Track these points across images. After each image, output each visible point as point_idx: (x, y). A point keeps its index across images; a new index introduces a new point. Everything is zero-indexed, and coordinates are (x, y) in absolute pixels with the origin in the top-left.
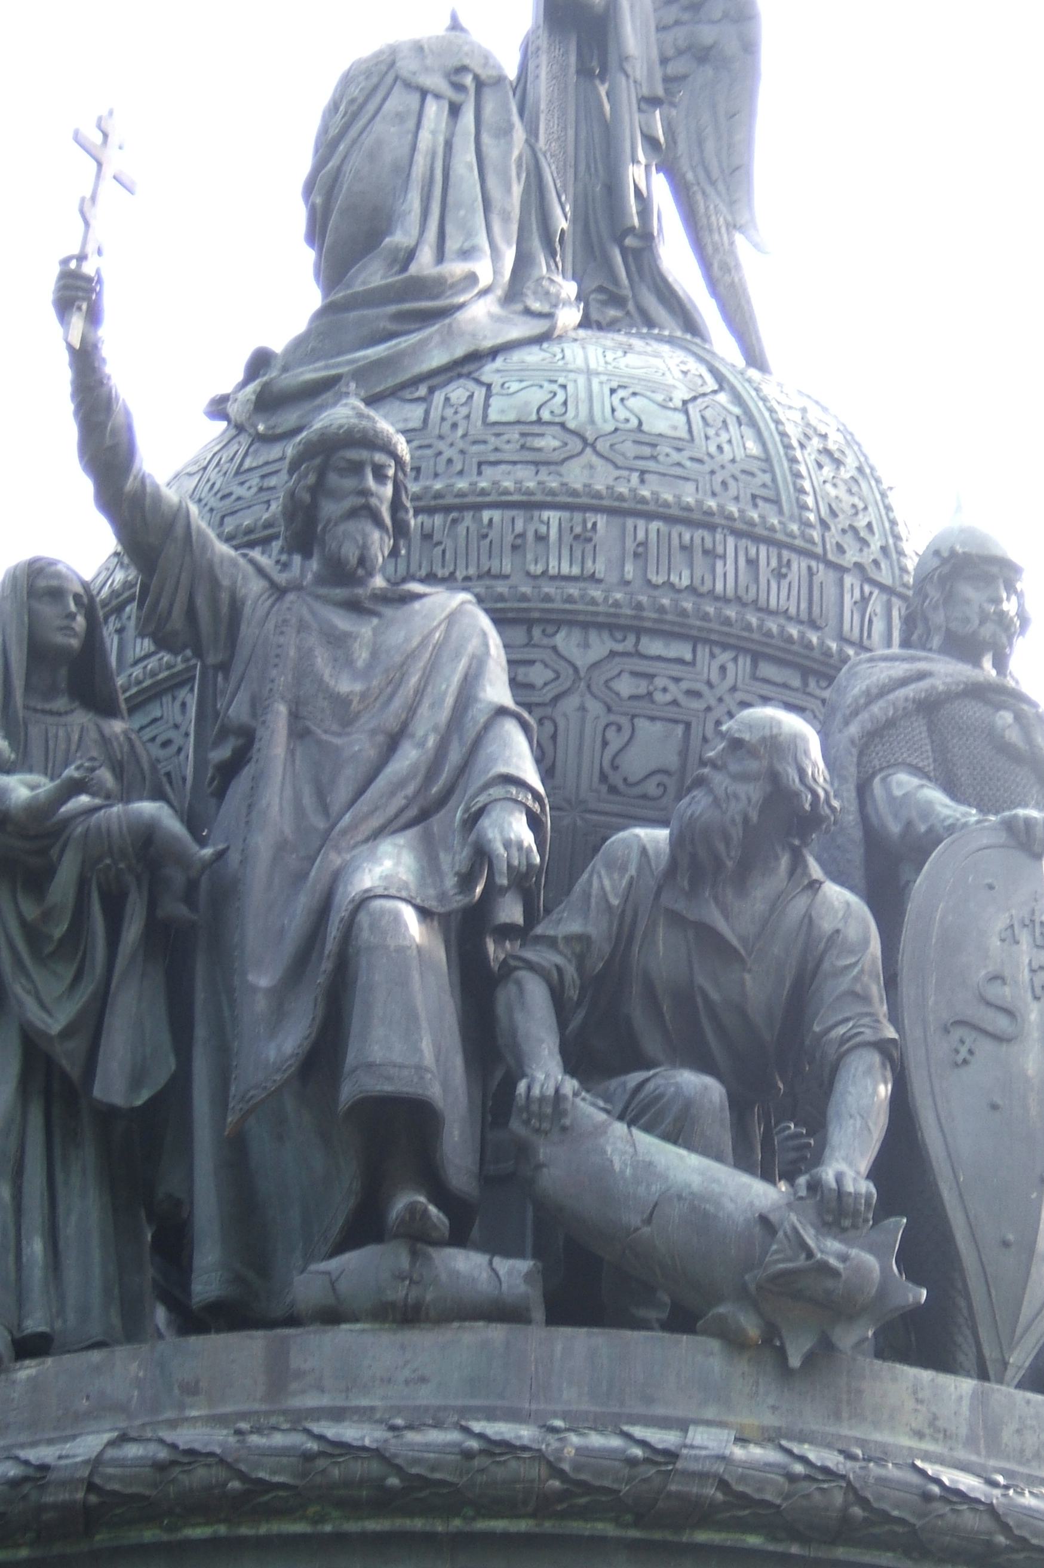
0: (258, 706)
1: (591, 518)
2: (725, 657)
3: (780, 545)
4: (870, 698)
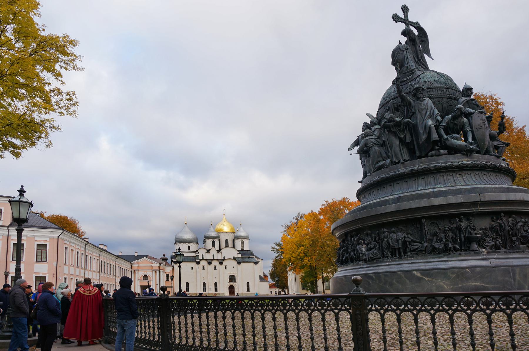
0: (415, 110)
1: (433, 89)
2: (445, 99)
3: (448, 89)
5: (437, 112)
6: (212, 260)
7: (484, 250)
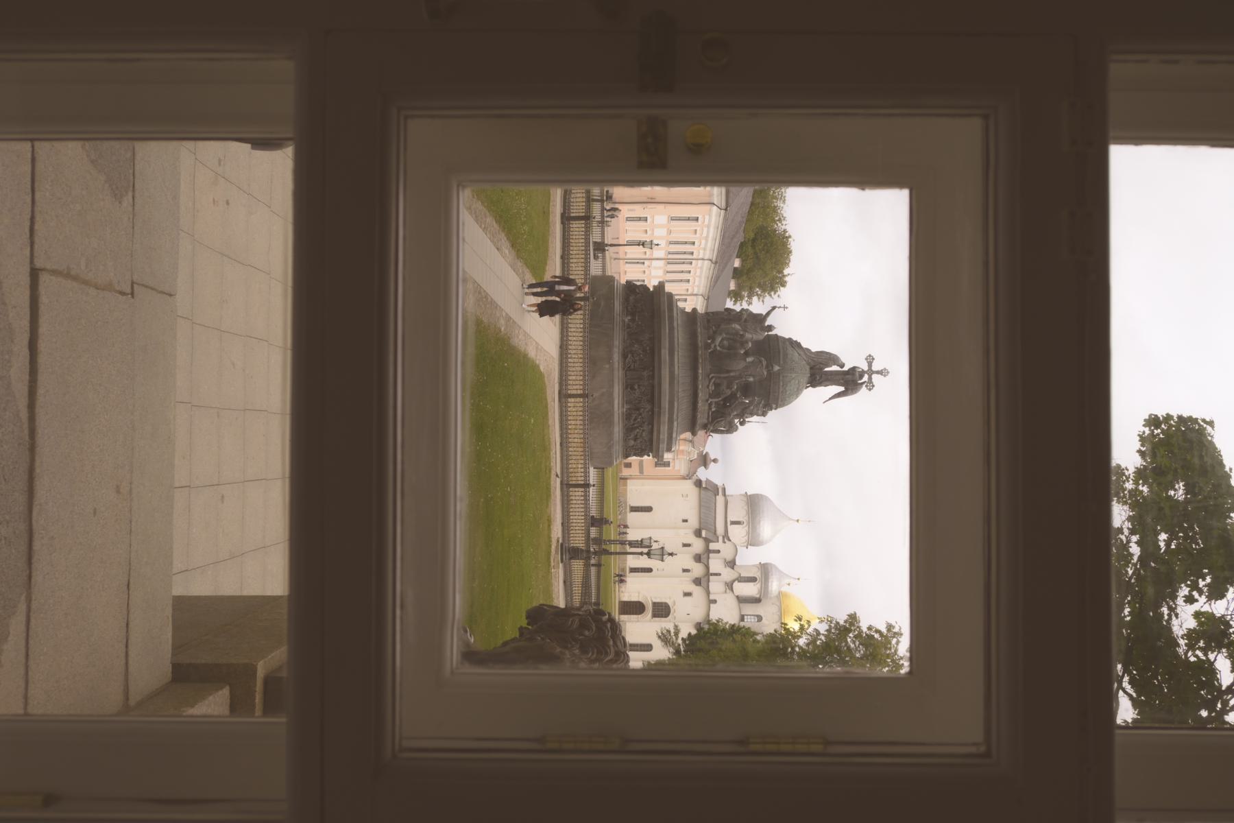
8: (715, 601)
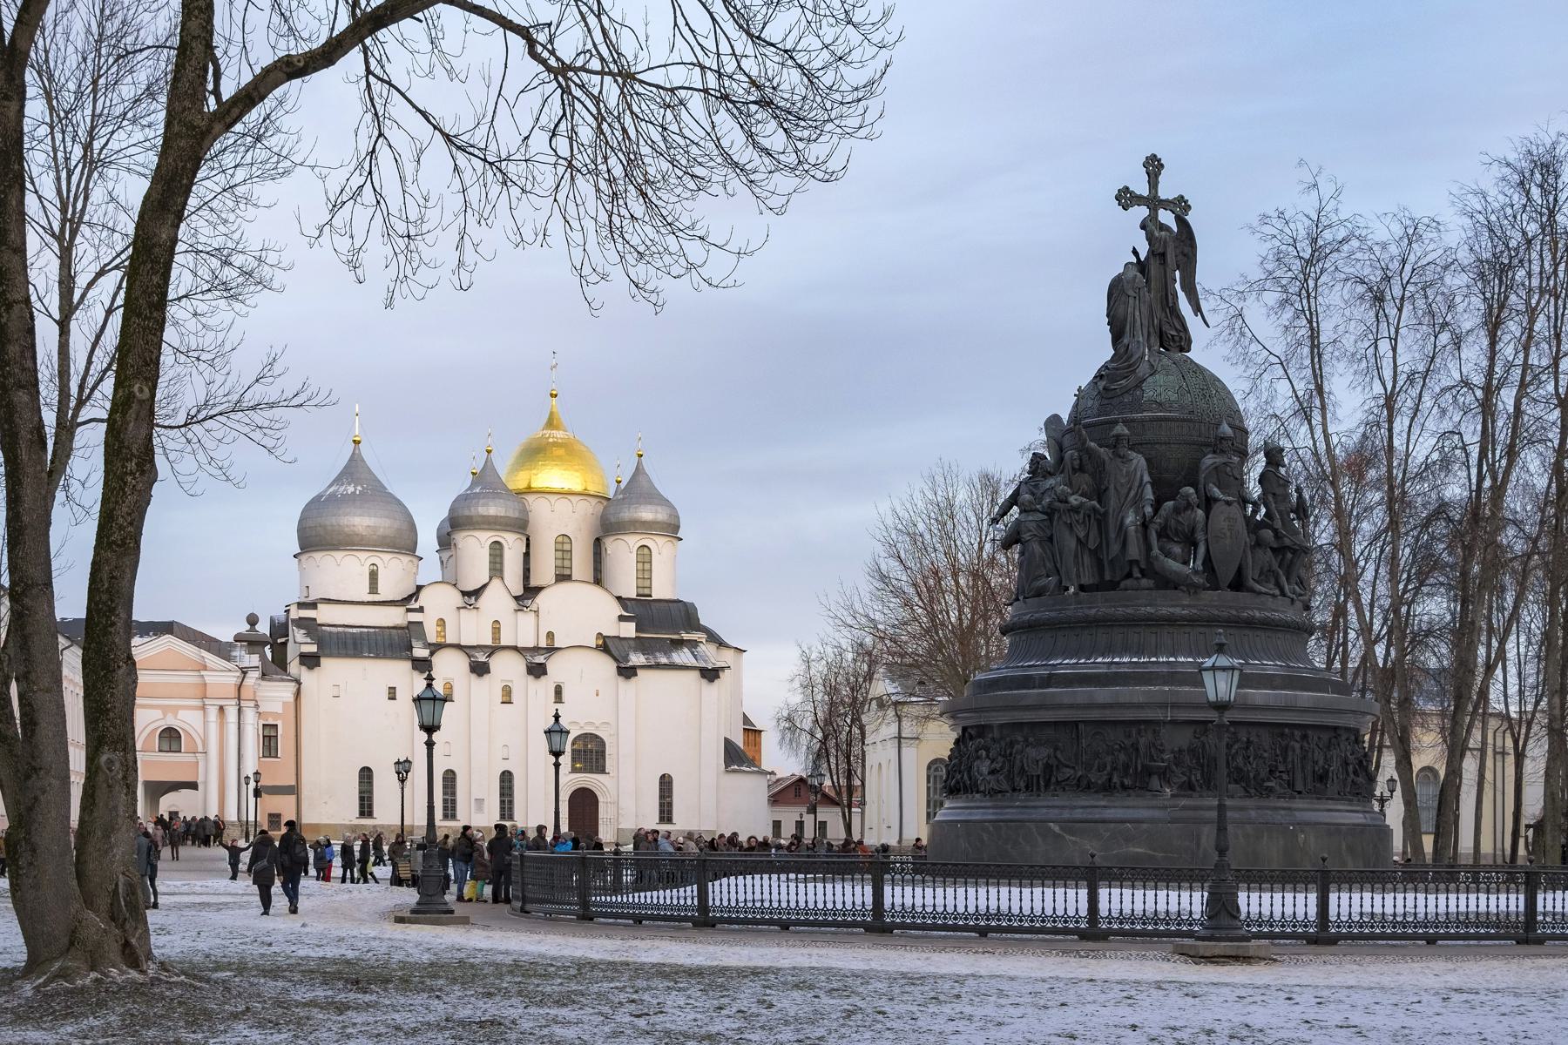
4: (1206, 469)
5: (1149, 494)
6: (493, 650)
7: (1168, 790)
8: (550, 635)
